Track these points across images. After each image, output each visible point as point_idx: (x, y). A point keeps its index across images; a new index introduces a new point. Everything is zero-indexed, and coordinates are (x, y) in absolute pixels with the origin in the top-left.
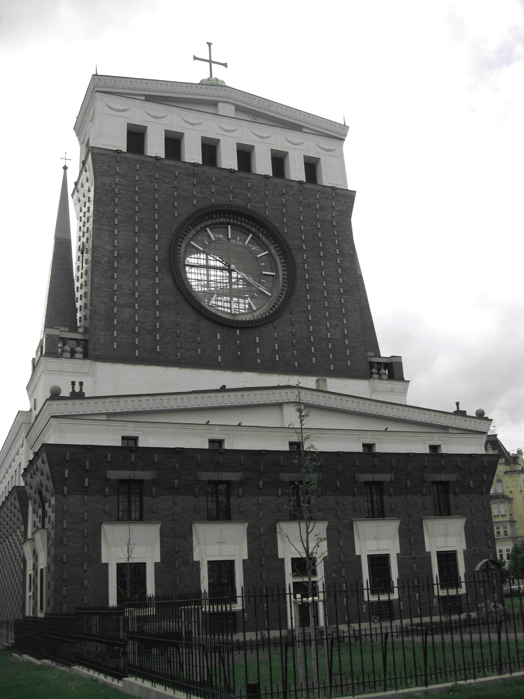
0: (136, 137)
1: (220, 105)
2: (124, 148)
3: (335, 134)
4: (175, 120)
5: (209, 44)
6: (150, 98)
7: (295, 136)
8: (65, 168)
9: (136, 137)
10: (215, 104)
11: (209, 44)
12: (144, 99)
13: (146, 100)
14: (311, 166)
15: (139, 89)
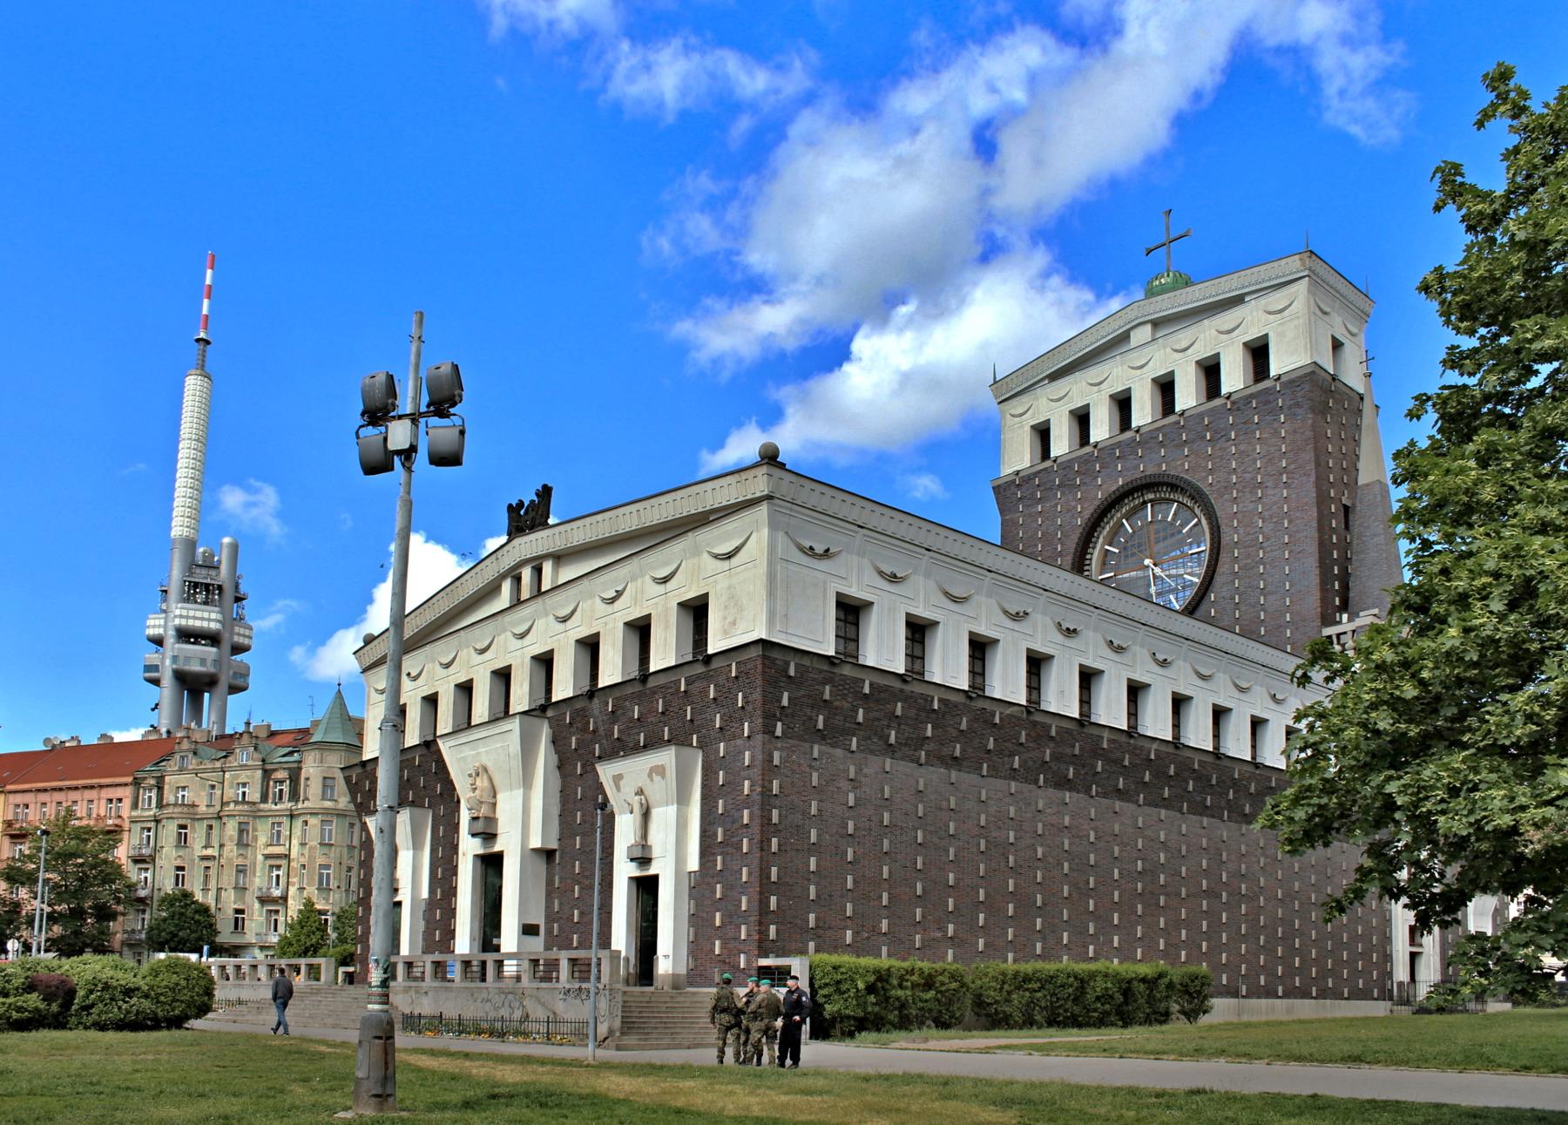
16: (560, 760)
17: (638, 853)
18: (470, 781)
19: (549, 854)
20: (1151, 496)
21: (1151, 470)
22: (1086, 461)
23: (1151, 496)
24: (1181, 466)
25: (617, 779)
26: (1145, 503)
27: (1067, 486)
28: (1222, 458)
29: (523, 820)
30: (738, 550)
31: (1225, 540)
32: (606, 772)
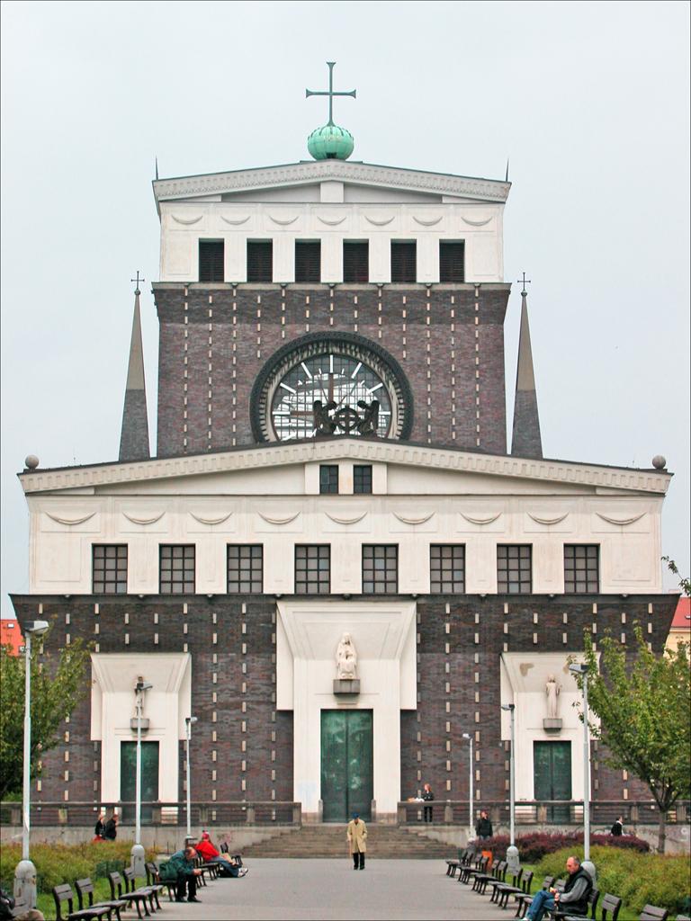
0: (211, 253)
1: (322, 186)
2: (192, 274)
3: (493, 194)
4: (259, 222)
5: (331, 65)
6: (226, 197)
7: (428, 212)
8: (138, 293)
9: (211, 253)
10: (318, 185)
11: (331, 65)
12: (219, 199)
13: (223, 201)
14: (452, 254)
15: (213, 189)
16: (421, 640)
17: (555, 726)
18: (342, 649)
19: (404, 713)
20: (337, 350)
21: (340, 328)
22: (273, 297)
23: (337, 350)
24: (377, 333)
25: (524, 668)
26: (327, 355)
27: (246, 315)
28: (416, 338)
29: (391, 688)
30: (632, 521)
31: (418, 412)
32: (511, 662)
